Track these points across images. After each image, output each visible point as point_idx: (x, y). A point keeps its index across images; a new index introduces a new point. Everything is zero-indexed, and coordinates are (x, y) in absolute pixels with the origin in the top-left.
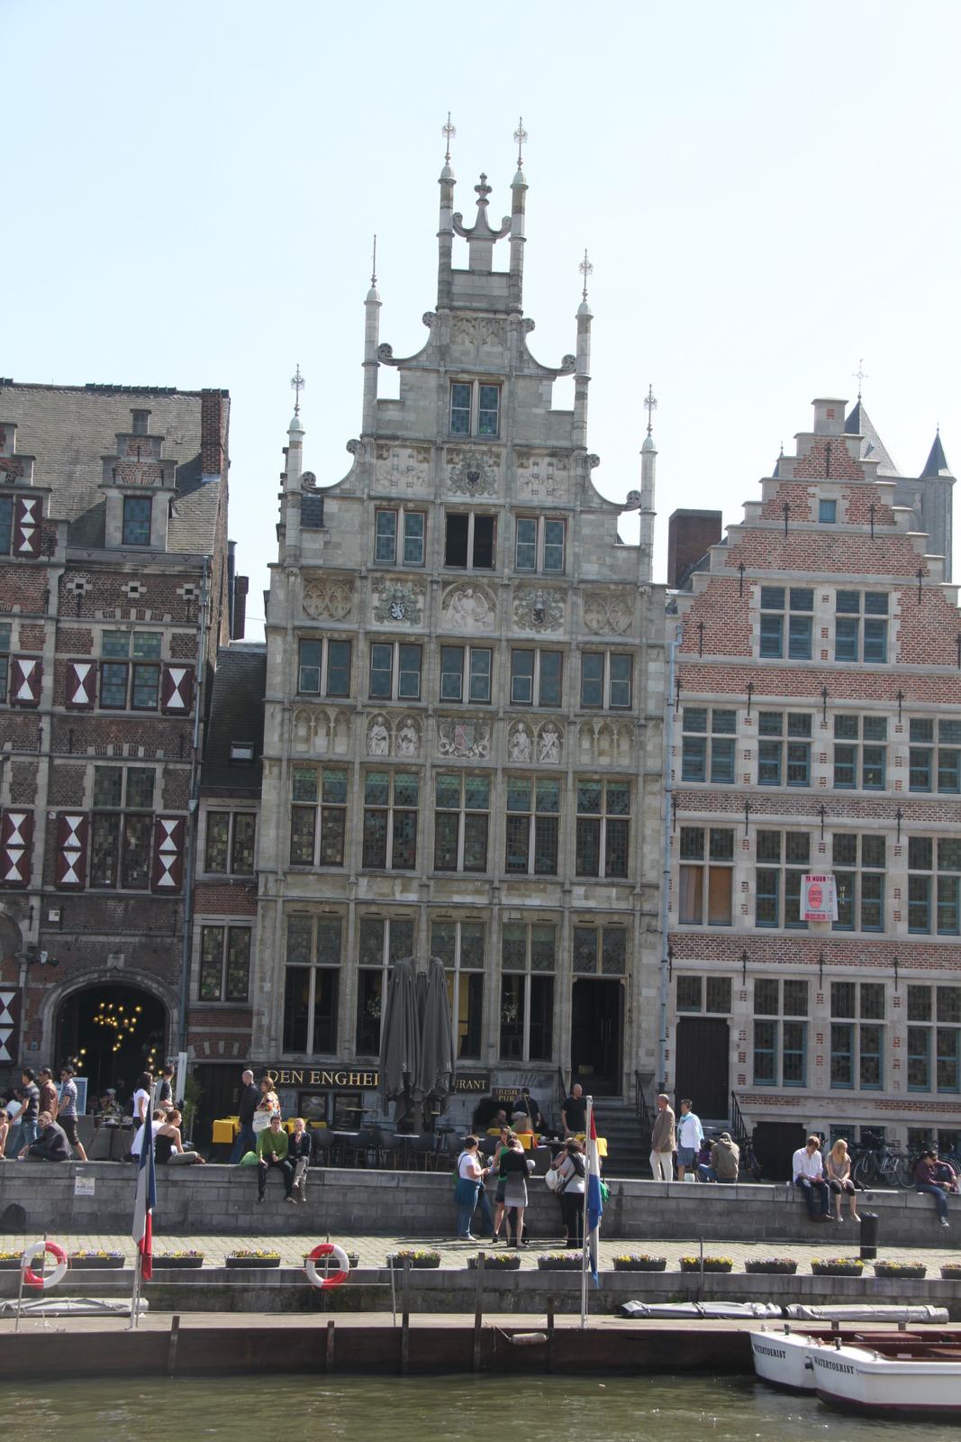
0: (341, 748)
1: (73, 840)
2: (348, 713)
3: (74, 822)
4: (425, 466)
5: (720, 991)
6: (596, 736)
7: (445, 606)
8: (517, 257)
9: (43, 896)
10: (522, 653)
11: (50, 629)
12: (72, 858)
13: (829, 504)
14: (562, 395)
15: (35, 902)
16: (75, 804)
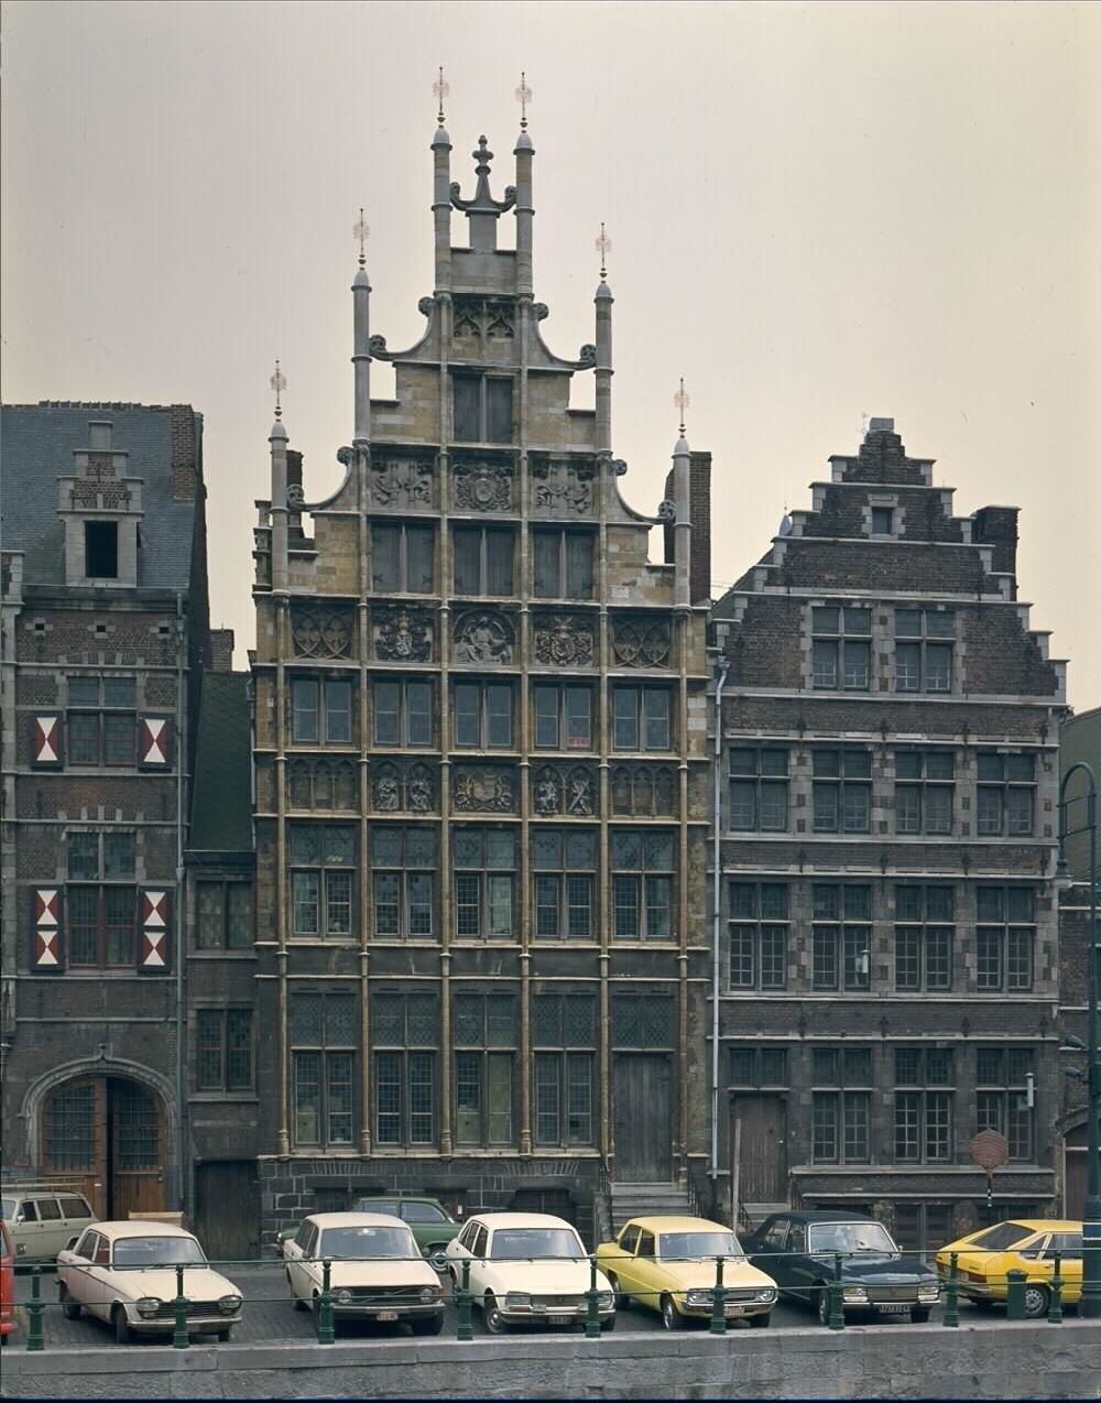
8: (524, 234)
14: (582, 391)
16: (47, 876)
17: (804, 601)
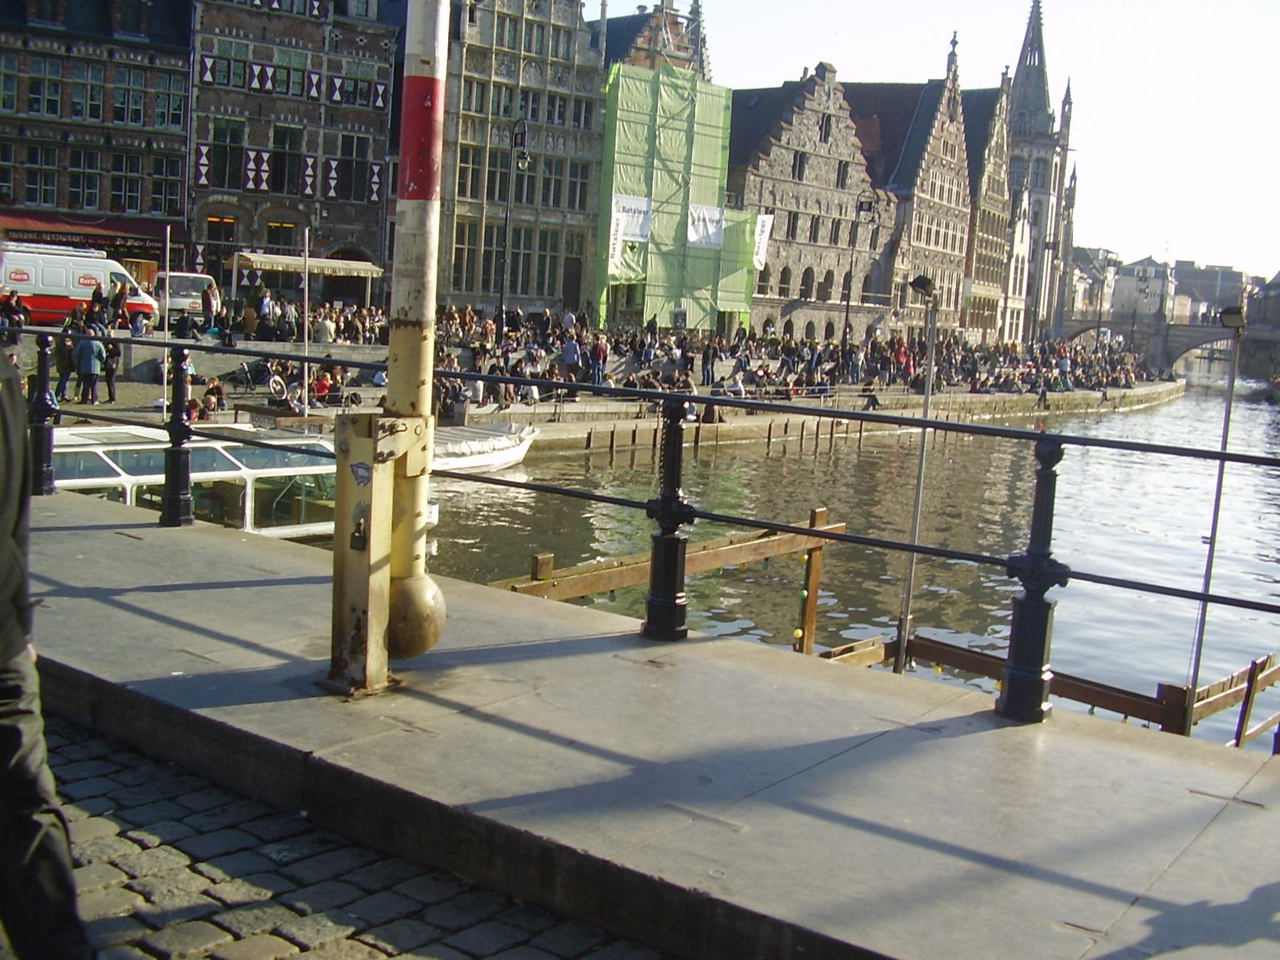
9: (321, 203)
10: (552, 98)
11: (325, 59)
12: (333, 183)
15: (318, 206)
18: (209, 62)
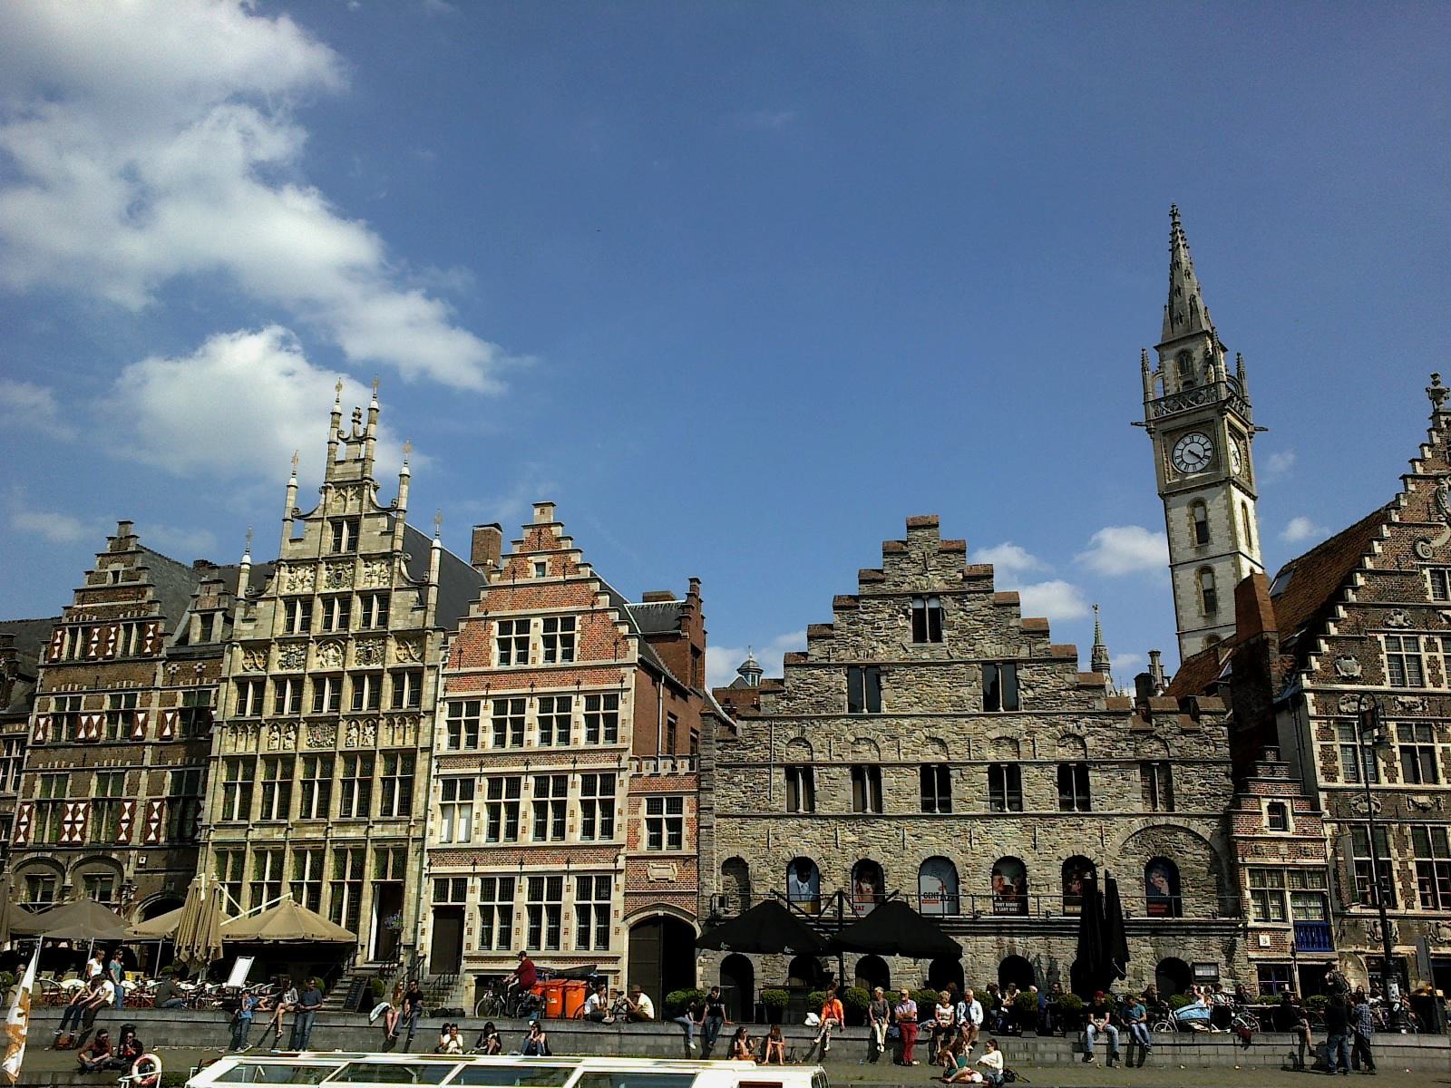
0: (252, 749)
1: (155, 816)
2: (257, 726)
3: (156, 805)
4: (312, 574)
5: (460, 885)
6: (396, 725)
7: (318, 655)
10: (357, 678)
13: (540, 566)
17: (494, 619)
18: (42, 721)
